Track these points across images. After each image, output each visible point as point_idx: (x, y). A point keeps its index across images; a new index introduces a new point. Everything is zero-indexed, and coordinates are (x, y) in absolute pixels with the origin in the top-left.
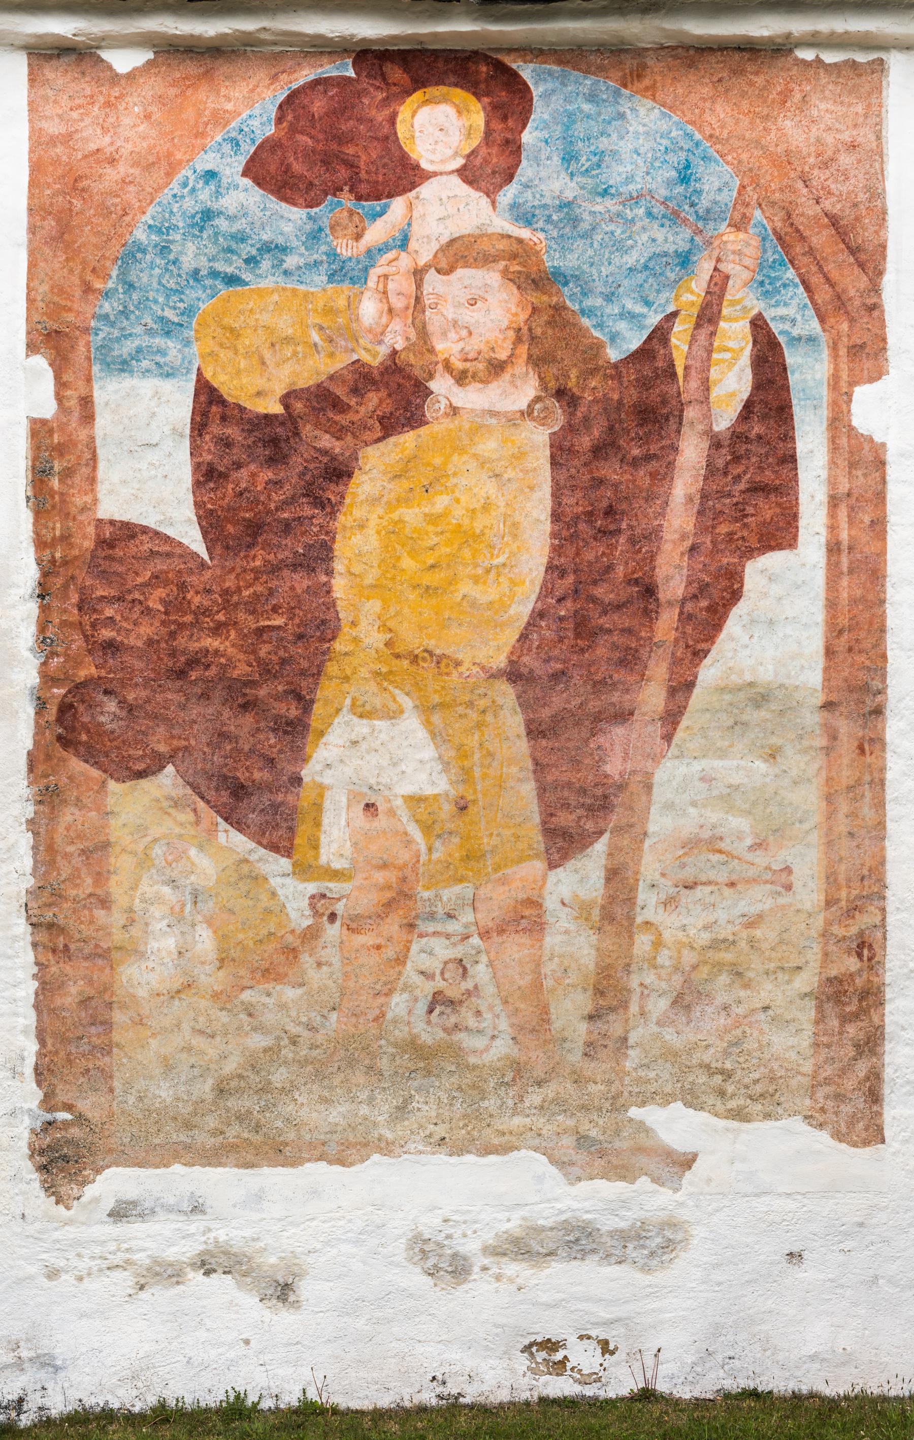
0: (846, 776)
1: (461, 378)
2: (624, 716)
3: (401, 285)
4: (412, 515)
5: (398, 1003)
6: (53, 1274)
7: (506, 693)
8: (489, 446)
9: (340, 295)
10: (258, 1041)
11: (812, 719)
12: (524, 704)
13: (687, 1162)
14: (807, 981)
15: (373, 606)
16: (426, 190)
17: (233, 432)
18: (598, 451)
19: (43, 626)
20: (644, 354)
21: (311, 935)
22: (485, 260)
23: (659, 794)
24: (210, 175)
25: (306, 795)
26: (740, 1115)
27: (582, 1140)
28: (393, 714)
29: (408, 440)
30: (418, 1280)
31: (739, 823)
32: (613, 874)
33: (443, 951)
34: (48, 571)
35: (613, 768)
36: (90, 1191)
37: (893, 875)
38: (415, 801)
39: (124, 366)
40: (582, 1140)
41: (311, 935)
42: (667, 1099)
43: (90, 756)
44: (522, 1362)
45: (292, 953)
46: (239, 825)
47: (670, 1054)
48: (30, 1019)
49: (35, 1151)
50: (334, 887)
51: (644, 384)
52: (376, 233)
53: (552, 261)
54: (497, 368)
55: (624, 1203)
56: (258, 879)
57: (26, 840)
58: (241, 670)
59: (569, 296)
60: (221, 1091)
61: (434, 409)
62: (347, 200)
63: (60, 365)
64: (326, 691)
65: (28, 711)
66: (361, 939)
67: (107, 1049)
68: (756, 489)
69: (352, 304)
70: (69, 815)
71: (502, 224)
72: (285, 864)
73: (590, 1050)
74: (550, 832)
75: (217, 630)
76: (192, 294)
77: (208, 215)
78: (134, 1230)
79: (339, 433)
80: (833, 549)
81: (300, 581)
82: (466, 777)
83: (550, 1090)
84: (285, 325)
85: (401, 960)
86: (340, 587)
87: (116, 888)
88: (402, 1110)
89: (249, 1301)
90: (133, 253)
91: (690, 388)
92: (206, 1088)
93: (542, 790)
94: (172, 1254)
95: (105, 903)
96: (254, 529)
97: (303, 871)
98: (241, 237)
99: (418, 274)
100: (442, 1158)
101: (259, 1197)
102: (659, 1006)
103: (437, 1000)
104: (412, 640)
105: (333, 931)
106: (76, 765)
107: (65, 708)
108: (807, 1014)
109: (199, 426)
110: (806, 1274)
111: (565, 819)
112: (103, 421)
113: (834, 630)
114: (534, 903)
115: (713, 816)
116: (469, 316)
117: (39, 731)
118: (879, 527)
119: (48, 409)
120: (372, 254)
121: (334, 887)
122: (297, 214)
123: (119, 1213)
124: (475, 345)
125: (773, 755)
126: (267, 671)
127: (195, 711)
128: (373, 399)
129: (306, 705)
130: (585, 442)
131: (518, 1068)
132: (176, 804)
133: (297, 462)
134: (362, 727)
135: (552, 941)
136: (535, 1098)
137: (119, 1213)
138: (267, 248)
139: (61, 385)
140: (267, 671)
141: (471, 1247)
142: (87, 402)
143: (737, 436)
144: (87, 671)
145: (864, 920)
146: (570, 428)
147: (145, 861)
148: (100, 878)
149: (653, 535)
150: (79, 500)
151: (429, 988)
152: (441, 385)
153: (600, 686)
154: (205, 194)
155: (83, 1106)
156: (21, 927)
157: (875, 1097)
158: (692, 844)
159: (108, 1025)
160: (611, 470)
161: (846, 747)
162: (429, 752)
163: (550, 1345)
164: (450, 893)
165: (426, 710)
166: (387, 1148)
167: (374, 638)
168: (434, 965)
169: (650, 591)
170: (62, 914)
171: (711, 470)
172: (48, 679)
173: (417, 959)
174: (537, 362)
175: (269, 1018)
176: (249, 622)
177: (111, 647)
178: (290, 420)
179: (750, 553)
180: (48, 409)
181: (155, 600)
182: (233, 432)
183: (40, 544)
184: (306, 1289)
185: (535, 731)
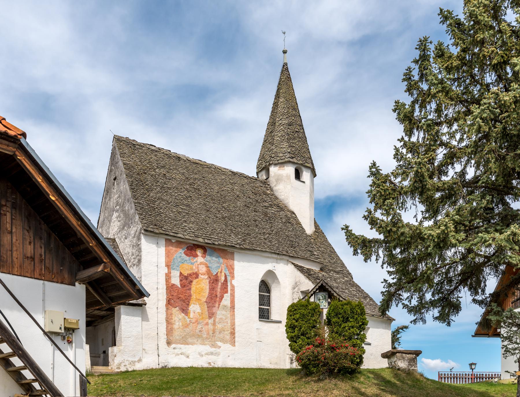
0: (232, 314)
1: (202, 275)
2: (215, 307)
3: (197, 265)
4: (198, 286)
5: (197, 331)
6: (168, 354)
7: (205, 304)
8: (204, 281)
9: (192, 266)
10: (185, 333)
11: (229, 309)
12: (207, 305)
13: (220, 347)
14: (229, 332)
15: (195, 294)
16: (199, 257)
17: (183, 277)
18: (213, 283)
19: (167, 292)
20: (216, 275)
21: (189, 324)
22: (204, 264)
23: (218, 314)
24: (181, 253)
25: (189, 311)
26: (224, 343)
27: (212, 345)
28: (197, 304)
29: (197, 279)
30: (199, 356)
31: (224, 317)
32: (214, 321)
33: (201, 327)
34: (167, 288)
35: (214, 311)
36: (172, 346)
37: (236, 323)
38: (198, 312)
39: (174, 269)
40: (212, 345)
41: (189, 324)
42: (219, 341)
43: (171, 305)
44: (207, 364)
45: (188, 325)
46: (183, 313)
47: (219, 337)
48: (165, 330)
49: (166, 342)
50: (192, 320)
51: (216, 277)
52: (195, 260)
53: (209, 265)
54: (204, 274)
55: (215, 350)
56: (185, 318)
57: (165, 313)
58: (184, 299)
59: (210, 268)
60: (182, 338)
61: (199, 277)
62: (192, 257)
63: (168, 268)
64: (191, 302)
65: (165, 300)
66: (194, 325)
67: (172, 333)
68: (225, 288)
69: (193, 267)
70: (169, 311)
71: (205, 261)
72: (187, 317)
73: (213, 336)
74: (209, 316)
75: (182, 295)
76: (180, 263)
77: (181, 256)
78: (175, 350)
79: (192, 278)
80: (231, 294)
81: (188, 291)
82: (202, 311)
83: (210, 340)
84: (187, 267)
85: (197, 327)
86: (192, 292)
87: (173, 318)
88: (197, 341)
89: (185, 358)
90: (174, 259)
91: (220, 278)
92: (181, 337)
93: (208, 312)
94: (178, 353)
95: (172, 319)
96: (185, 286)
97: (189, 318)
98: (183, 259)
99: (198, 265)
100: (201, 345)
101: (186, 348)
102: (218, 333)
103: (200, 331)
104: (198, 298)
105: (191, 324)
106: (170, 306)
107: (169, 301)
108: (229, 335)
109: (180, 276)
110: (230, 358)
111: (210, 315)
112: (172, 274)
113: (231, 301)
114: (208, 323)
115: (222, 316)
116: (202, 269)
117: (166, 302)
118: (234, 292)
119: (167, 272)
120: (194, 262)
121: (192, 320)
122: (188, 258)
123: (174, 348)
124: (203, 272)
125: (226, 311)
126: (186, 299)
127: (180, 302)
128: (194, 275)
129: (189, 303)
130: (211, 282)
131: (207, 338)
132: (178, 310)
133: (188, 280)
134: (194, 305)
135: (209, 326)
136: (208, 340)
137: (174, 348)
138: (186, 260)
139: (168, 270)
140: (186, 299)
141: (203, 354)
142: (170, 272)
143: (223, 283)
144: (170, 297)
145: (234, 327)
146: (210, 280)
147: (175, 315)
148: (172, 317)
149: (217, 291)
150: (170, 281)
151: (199, 330)
152: (200, 275)
153: (213, 304)
154: (180, 254)
155: (170, 338)
156: (165, 321)
157: (235, 342)
158: (220, 319)
159: (172, 331)
160: (213, 285)
161: (232, 311)
162: (199, 308)
163: (210, 363)
164: (201, 321)
165: (199, 304)
166: (196, 344)
167: (195, 297)
168: (200, 327)
169: (217, 296)
170: (168, 320)
171: (221, 286)
172: (167, 298)
173: (198, 327)
174: (208, 274)
175: (186, 331)
176: (184, 295)
177: (173, 295)
178: (188, 276)
179: (224, 293)
180: (167, 272)
181: (176, 291)
182: (183, 277)
183: (166, 285)
184: (190, 357)
185: (208, 307)
